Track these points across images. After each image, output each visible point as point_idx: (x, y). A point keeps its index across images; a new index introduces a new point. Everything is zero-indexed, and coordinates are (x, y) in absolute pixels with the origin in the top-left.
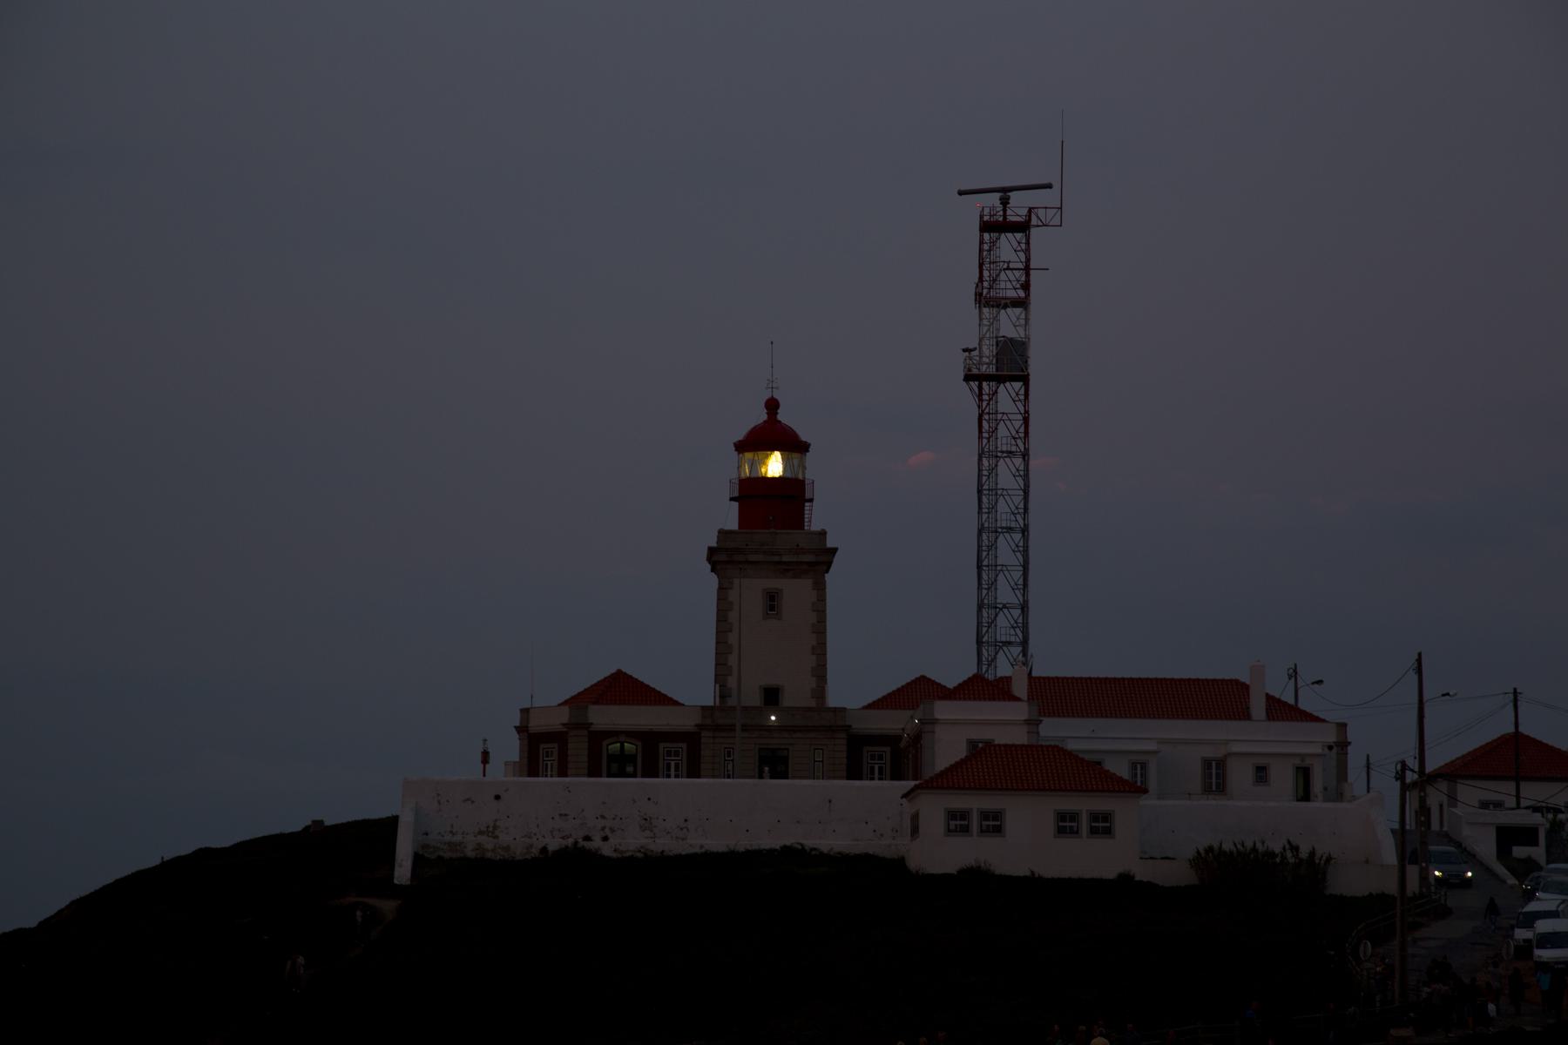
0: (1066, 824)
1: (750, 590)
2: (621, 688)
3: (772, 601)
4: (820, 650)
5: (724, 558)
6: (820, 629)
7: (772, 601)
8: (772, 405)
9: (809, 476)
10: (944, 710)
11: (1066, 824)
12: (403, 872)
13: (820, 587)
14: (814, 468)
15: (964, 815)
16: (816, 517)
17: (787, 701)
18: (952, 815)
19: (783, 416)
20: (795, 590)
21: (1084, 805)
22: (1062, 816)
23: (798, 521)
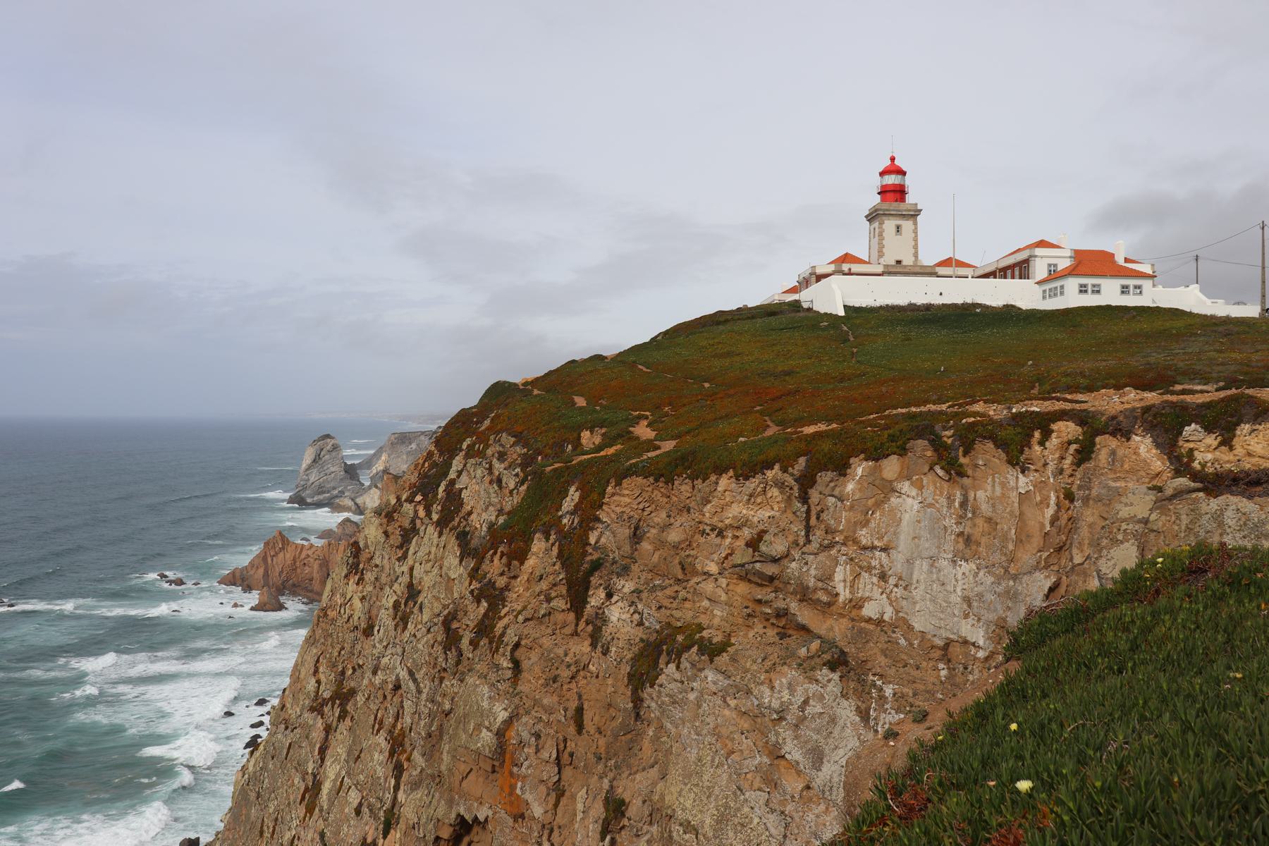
0: (1125, 290)
1: (890, 225)
2: (847, 258)
3: (898, 228)
4: (916, 247)
5: (873, 216)
6: (916, 240)
7: (898, 228)
8: (893, 159)
9: (907, 183)
10: (1039, 251)
11: (1125, 290)
12: (842, 313)
13: (915, 224)
14: (909, 181)
15: (1085, 286)
16: (910, 199)
17: (904, 263)
18: (1081, 286)
19: (896, 162)
20: (907, 225)
21: (1131, 282)
22: (1123, 287)
23: (903, 200)
